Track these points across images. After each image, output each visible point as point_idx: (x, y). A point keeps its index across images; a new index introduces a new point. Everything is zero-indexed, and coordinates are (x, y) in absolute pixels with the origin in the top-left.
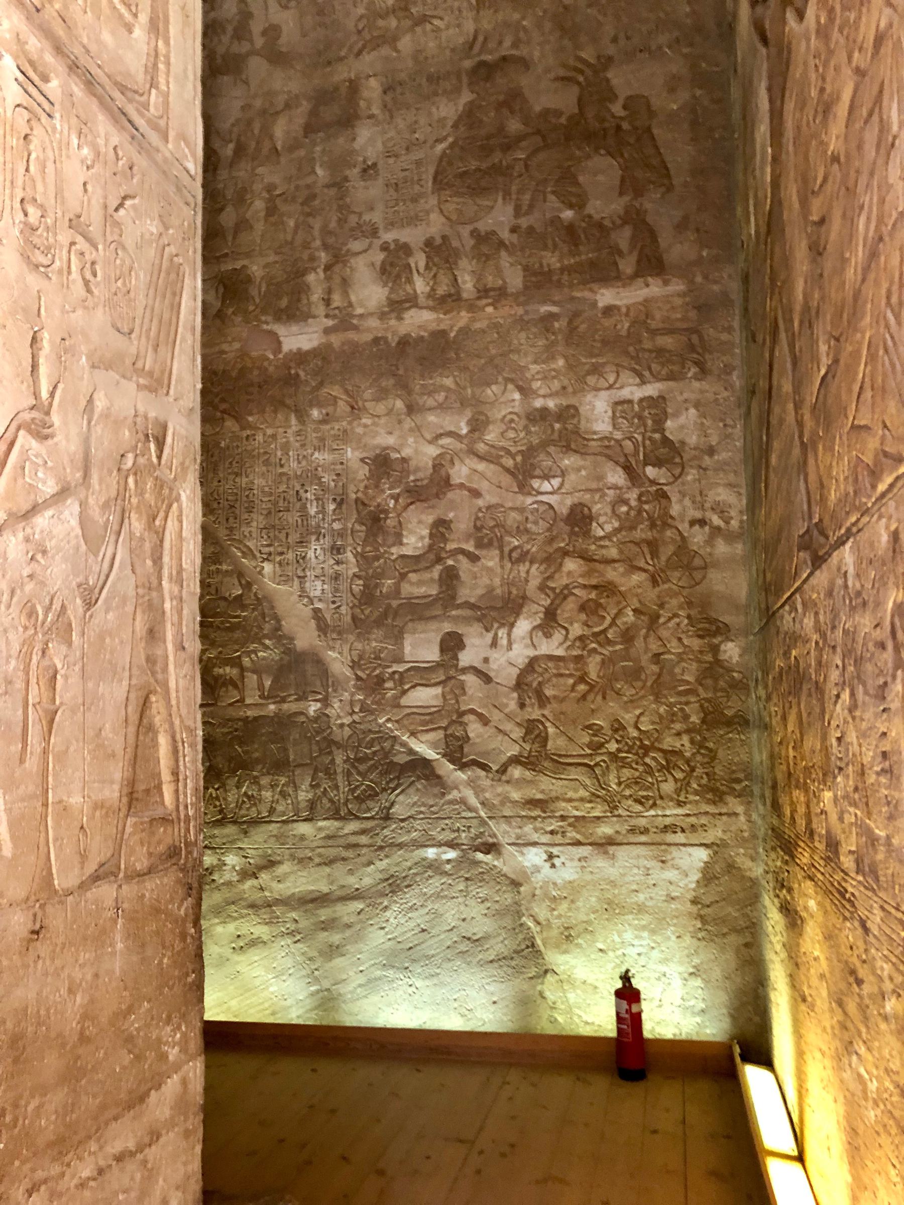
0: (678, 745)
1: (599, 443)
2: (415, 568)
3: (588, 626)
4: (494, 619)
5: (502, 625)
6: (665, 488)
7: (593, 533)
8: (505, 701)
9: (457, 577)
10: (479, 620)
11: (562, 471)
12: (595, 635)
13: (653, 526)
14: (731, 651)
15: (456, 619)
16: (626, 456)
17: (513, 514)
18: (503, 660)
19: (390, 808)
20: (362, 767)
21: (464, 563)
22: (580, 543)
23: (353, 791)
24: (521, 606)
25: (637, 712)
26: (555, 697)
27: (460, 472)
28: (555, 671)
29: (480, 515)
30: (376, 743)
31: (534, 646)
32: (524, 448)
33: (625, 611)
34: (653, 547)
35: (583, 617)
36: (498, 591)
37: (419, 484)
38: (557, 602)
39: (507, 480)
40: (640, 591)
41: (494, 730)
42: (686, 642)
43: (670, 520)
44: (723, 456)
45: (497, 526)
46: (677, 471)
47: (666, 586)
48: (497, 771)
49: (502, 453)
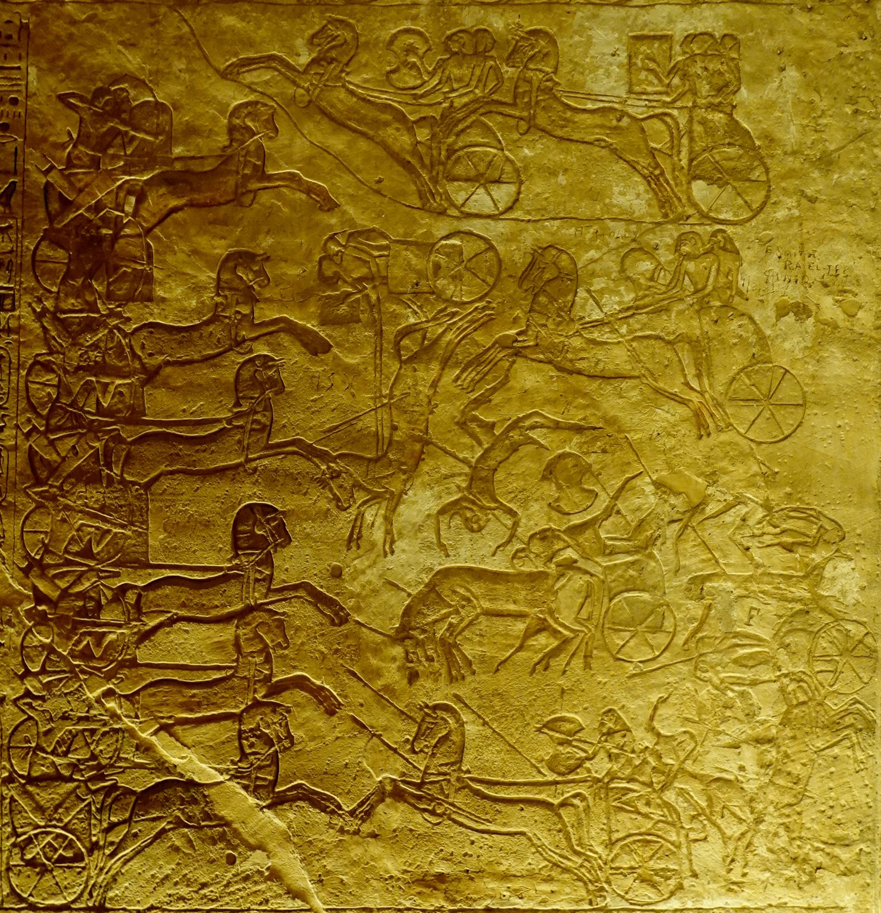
0: (733, 767)
1: (597, 119)
2: (182, 355)
3: (559, 510)
4: (357, 485)
5: (376, 497)
6: (730, 230)
7: (577, 312)
8: (374, 662)
9: (277, 385)
10: (323, 483)
11: (517, 171)
12: (576, 530)
13: (703, 307)
14: (845, 579)
15: (272, 479)
16: (652, 152)
17: (411, 256)
18: (372, 575)
19: (108, 887)
20: (44, 797)
21: (292, 358)
22: (549, 332)
23: (23, 848)
24: (419, 460)
25: (654, 698)
26: (483, 659)
27: (293, 148)
28: (486, 605)
29: (335, 248)
30: (78, 743)
31: (442, 546)
32: (436, 113)
33: (638, 482)
34: (701, 350)
35: (550, 490)
36: (369, 423)
37: (195, 166)
38: (498, 454)
39: (394, 177)
40: (671, 442)
41: (349, 724)
42: (756, 553)
43: (737, 299)
44: (850, 176)
45: (369, 278)
46: (756, 198)
47: (724, 437)
48: (352, 813)
49: (387, 117)
